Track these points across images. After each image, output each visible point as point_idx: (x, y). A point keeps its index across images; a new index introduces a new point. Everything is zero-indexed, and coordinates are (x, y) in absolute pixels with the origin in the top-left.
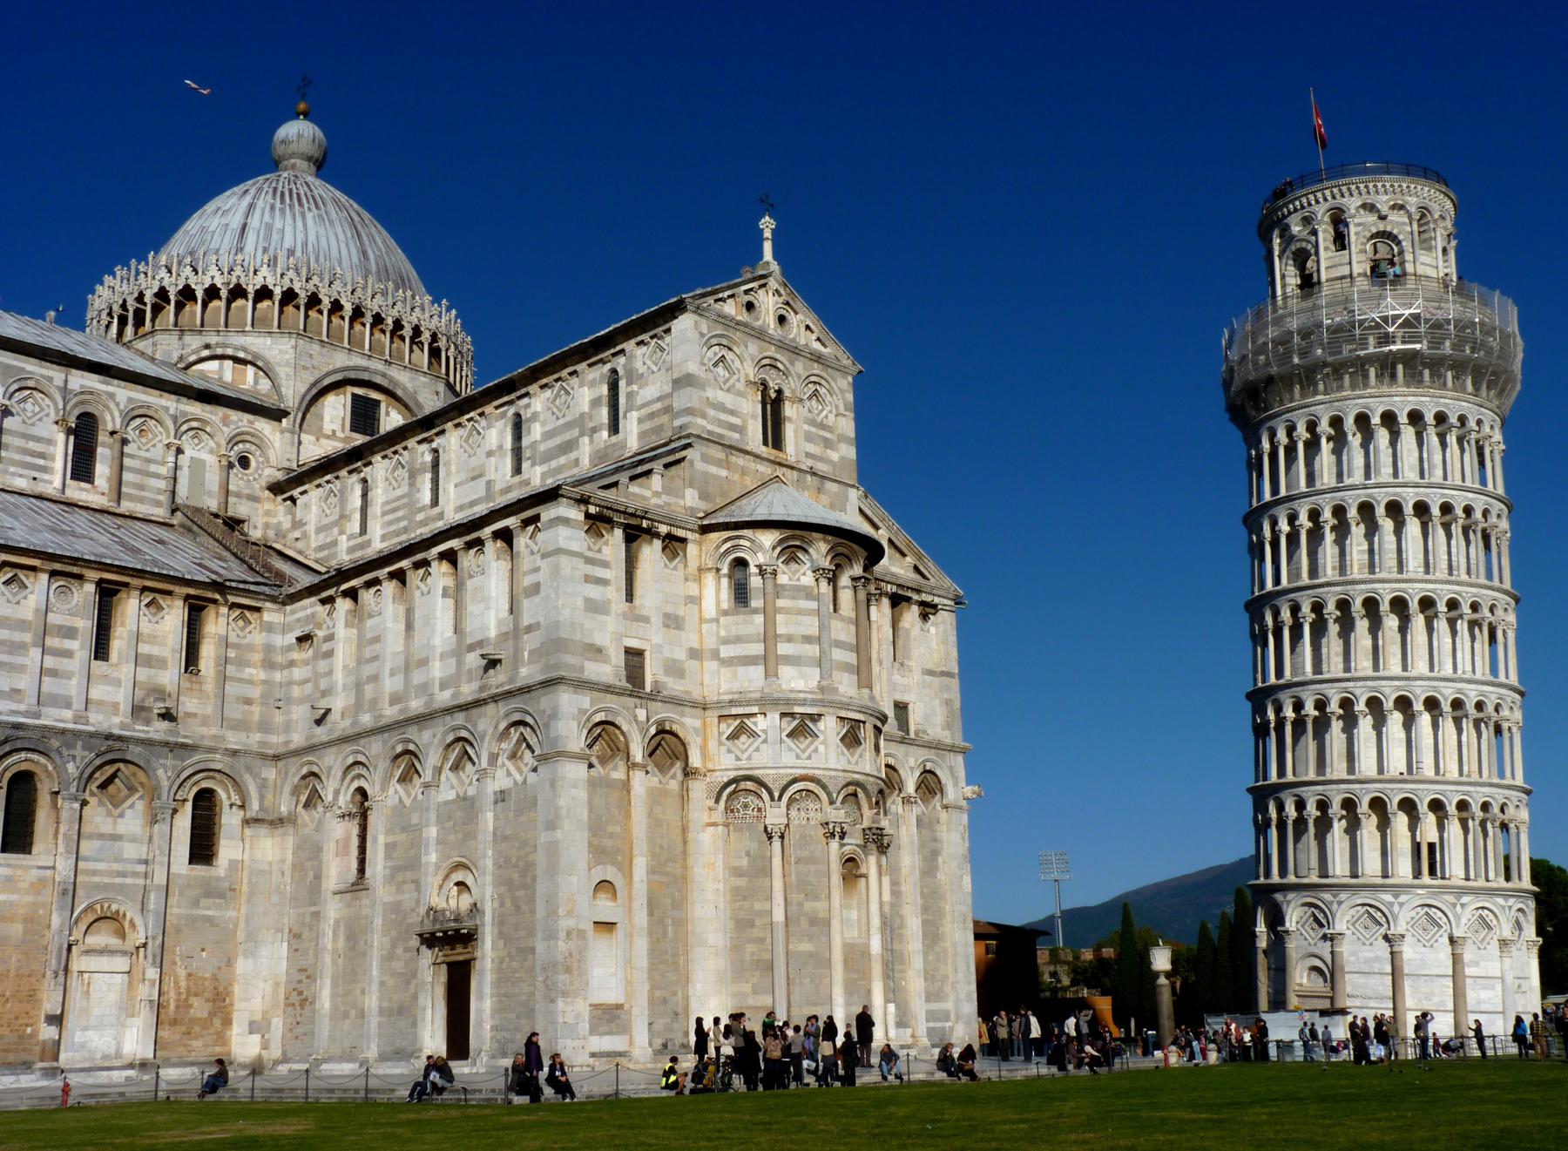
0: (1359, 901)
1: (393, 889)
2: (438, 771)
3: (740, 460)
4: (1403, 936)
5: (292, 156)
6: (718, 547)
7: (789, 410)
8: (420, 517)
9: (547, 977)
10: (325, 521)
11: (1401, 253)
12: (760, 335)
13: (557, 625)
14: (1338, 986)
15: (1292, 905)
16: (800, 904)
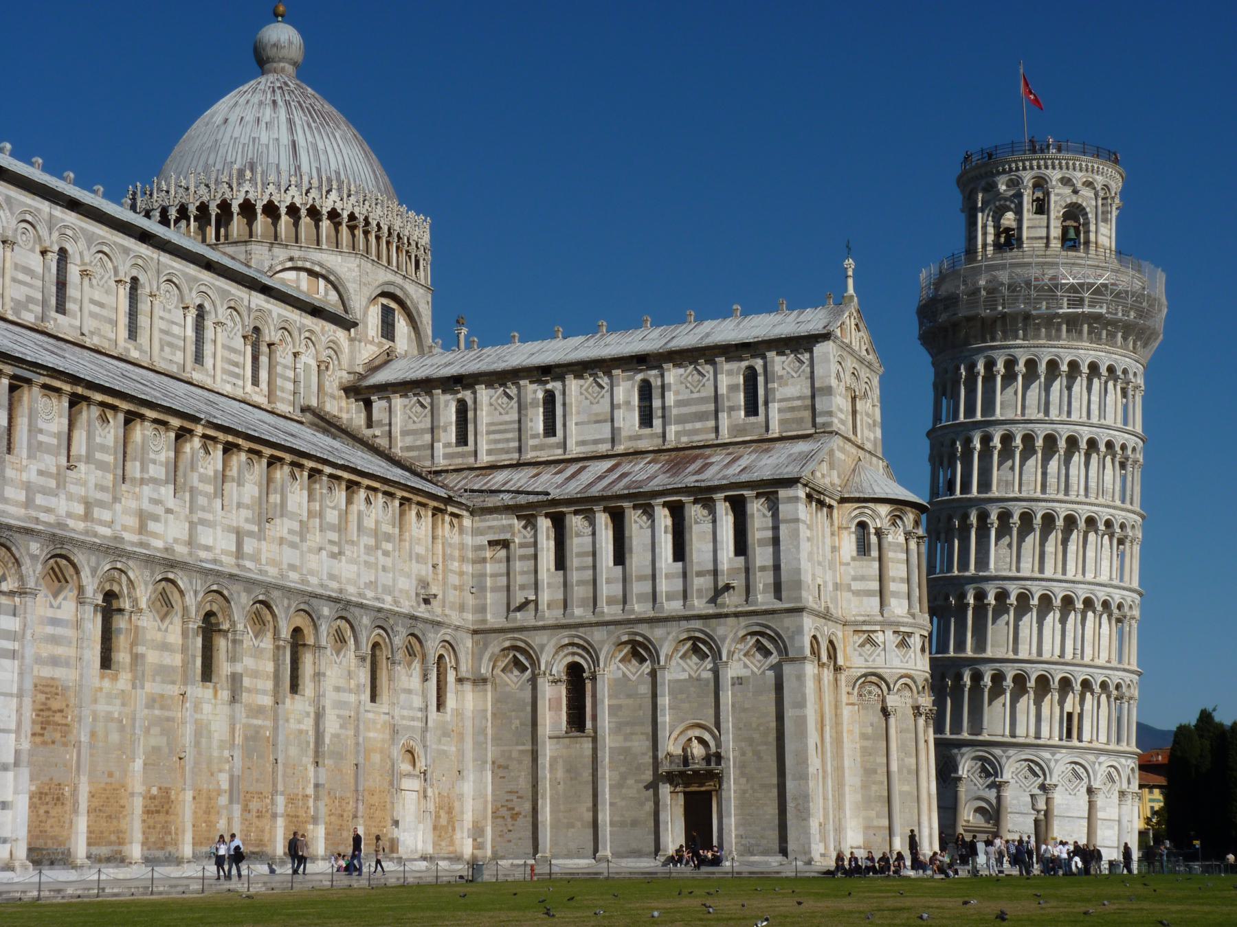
0: (1024, 757)
1: (621, 738)
2: (669, 657)
3: (848, 446)
4: (1056, 786)
5: (282, 60)
6: (850, 513)
7: (859, 405)
8: (531, 442)
9: (798, 804)
10: (412, 427)
11: (1087, 224)
12: (852, 353)
13: (798, 571)
14: (1003, 824)
15: (965, 757)
16: (903, 760)
